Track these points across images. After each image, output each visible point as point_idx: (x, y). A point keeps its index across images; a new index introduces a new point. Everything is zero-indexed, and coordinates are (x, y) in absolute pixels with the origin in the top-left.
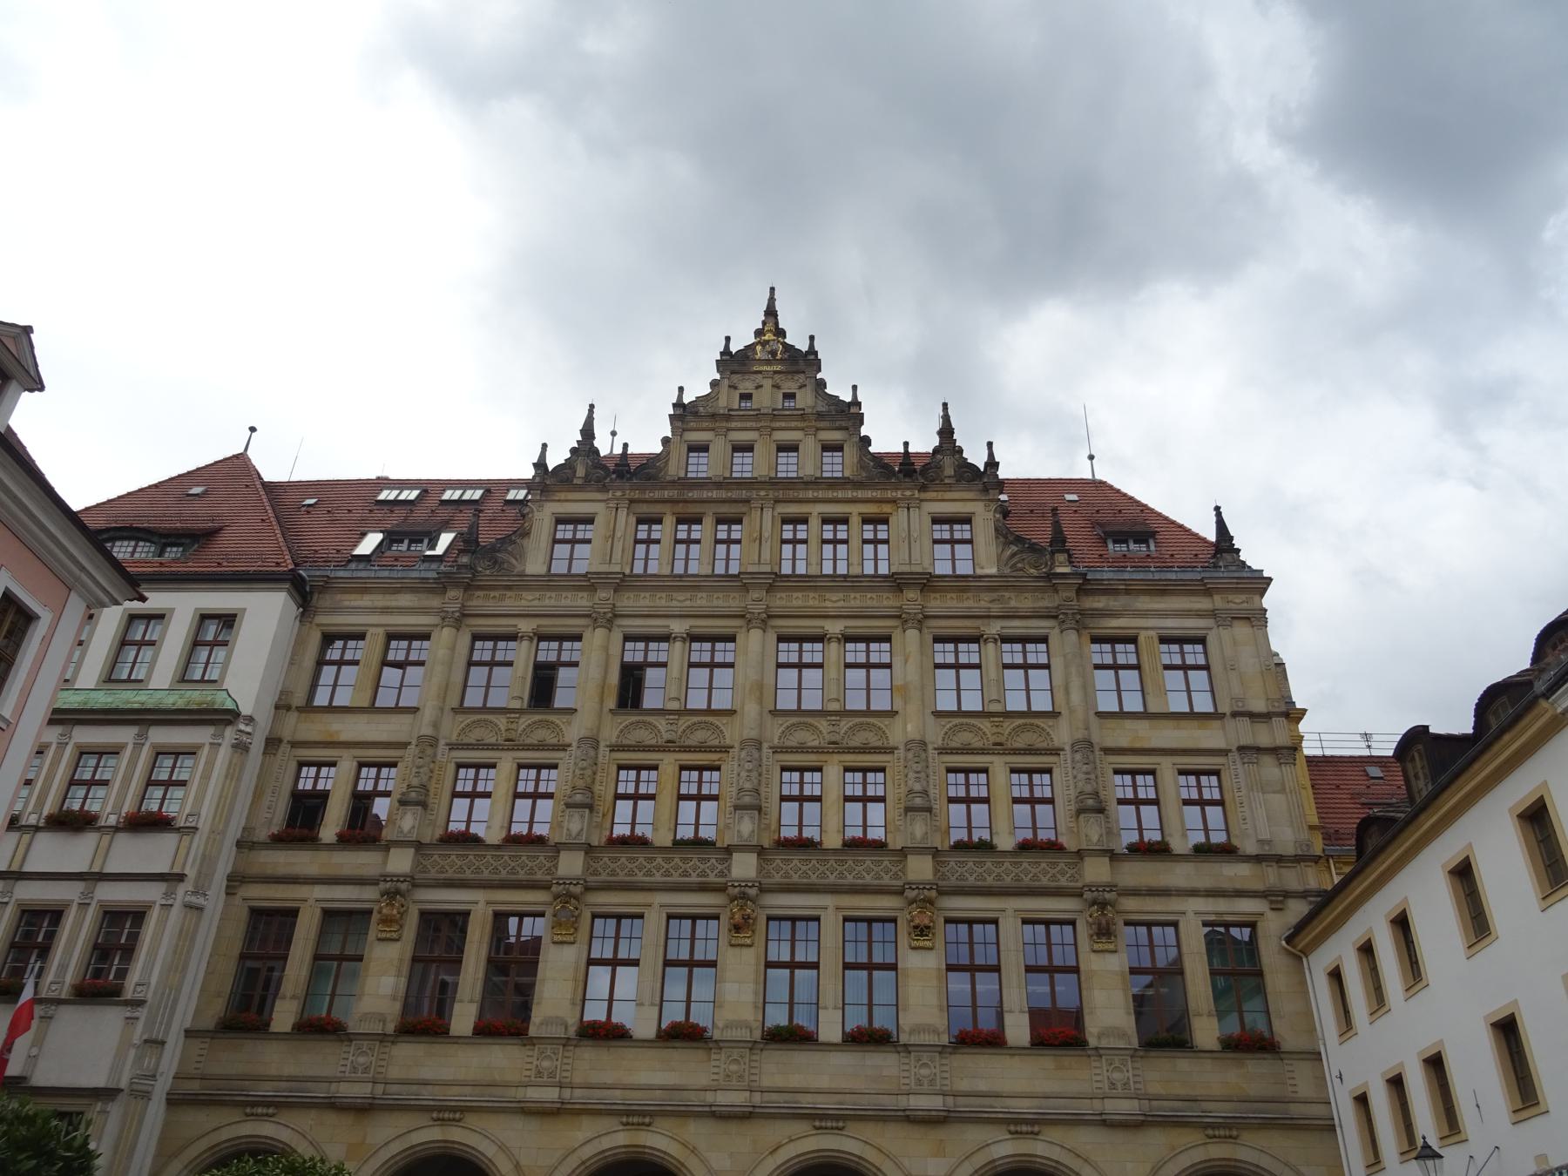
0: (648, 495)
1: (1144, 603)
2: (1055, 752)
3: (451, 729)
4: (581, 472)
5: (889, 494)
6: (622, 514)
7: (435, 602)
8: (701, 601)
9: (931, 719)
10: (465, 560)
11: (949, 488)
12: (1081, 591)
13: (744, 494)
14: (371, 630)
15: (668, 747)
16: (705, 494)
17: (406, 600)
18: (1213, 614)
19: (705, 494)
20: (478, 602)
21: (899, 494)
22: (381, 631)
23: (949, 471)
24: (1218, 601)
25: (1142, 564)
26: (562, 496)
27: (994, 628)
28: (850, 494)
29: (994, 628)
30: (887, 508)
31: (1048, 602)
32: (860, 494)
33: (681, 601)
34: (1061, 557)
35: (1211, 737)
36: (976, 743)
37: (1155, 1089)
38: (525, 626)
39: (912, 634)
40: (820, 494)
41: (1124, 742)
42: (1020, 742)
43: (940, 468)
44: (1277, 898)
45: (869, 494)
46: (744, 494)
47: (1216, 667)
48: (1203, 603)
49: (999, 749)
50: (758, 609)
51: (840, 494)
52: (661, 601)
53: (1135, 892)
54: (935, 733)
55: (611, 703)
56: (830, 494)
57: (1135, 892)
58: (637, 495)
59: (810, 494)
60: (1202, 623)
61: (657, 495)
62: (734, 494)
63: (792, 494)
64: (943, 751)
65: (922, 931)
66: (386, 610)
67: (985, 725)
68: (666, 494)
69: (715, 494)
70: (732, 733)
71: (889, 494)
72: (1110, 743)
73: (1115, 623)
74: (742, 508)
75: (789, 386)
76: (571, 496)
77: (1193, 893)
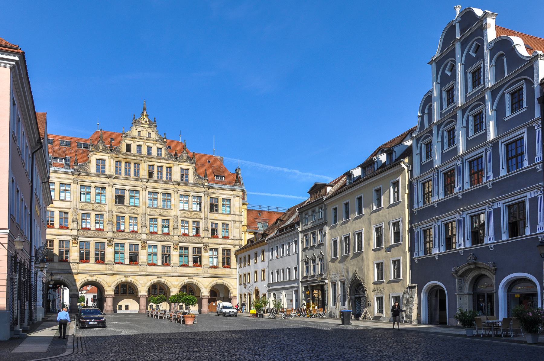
0: (118, 156)
1: (220, 191)
2: (201, 219)
3: (80, 205)
4: (101, 148)
5: (172, 162)
6: (112, 160)
7: (71, 177)
8: (132, 183)
9: (178, 211)
10: (76, 167)
11: (184, 162)
12: (209, 189)
13: (140, 158)
14: (56, 182)
15: (127, 213)
16: (131, 157)
17: (63, 176)
18: (233, 195)
19: (131, 157)
20: (81, 178)
21: (174, 162)
22: (59, 183)
23: (185, 158)
24: (234, 193)
25: (222, 183)
26: (97, 153)
27: (192, 194)
28: (163, 161)
29: (192, 194)
30: (171, 165)
31: (203, 190)
32: (166, 162)
33: (128, 182)
34: (206, 180)
35: (229, 218)
36: (187, 216)
37: (211, 273)
38: (93, 185)
39: (176, 194)
40: (157, 161)
41: (213, 218)
42: (195, 216)
43: (183, 157)
44: (234, 245)
45: (167, 162)
46: (140, 158)
47: (232, 205)
48: (231, 193)
49: (191, 217)
50: (144, 186)
51: (162, 161)
52: (123, 182)
53: (212, 244)
54: (179, 213)
55: (114, 203)
56: (159, 161)
57: (212, 244)
58: (115, 155)
59: (155, 160)
60: (230, 197)
61: (120, 156)
62: (138, 158)
63: (151, 160)
64: (180, 217)
65: (176, 249)
66: (59, 178)
67: (189, 213)
68: (122, 156)
69: (134, 158)
70: (140, 210)
71: (172, 162)
72: (211, 218)
73: (214, 195)
74: (140, 162)
75: (150, 131)
76: (99, 154)
77: (221, 244)
